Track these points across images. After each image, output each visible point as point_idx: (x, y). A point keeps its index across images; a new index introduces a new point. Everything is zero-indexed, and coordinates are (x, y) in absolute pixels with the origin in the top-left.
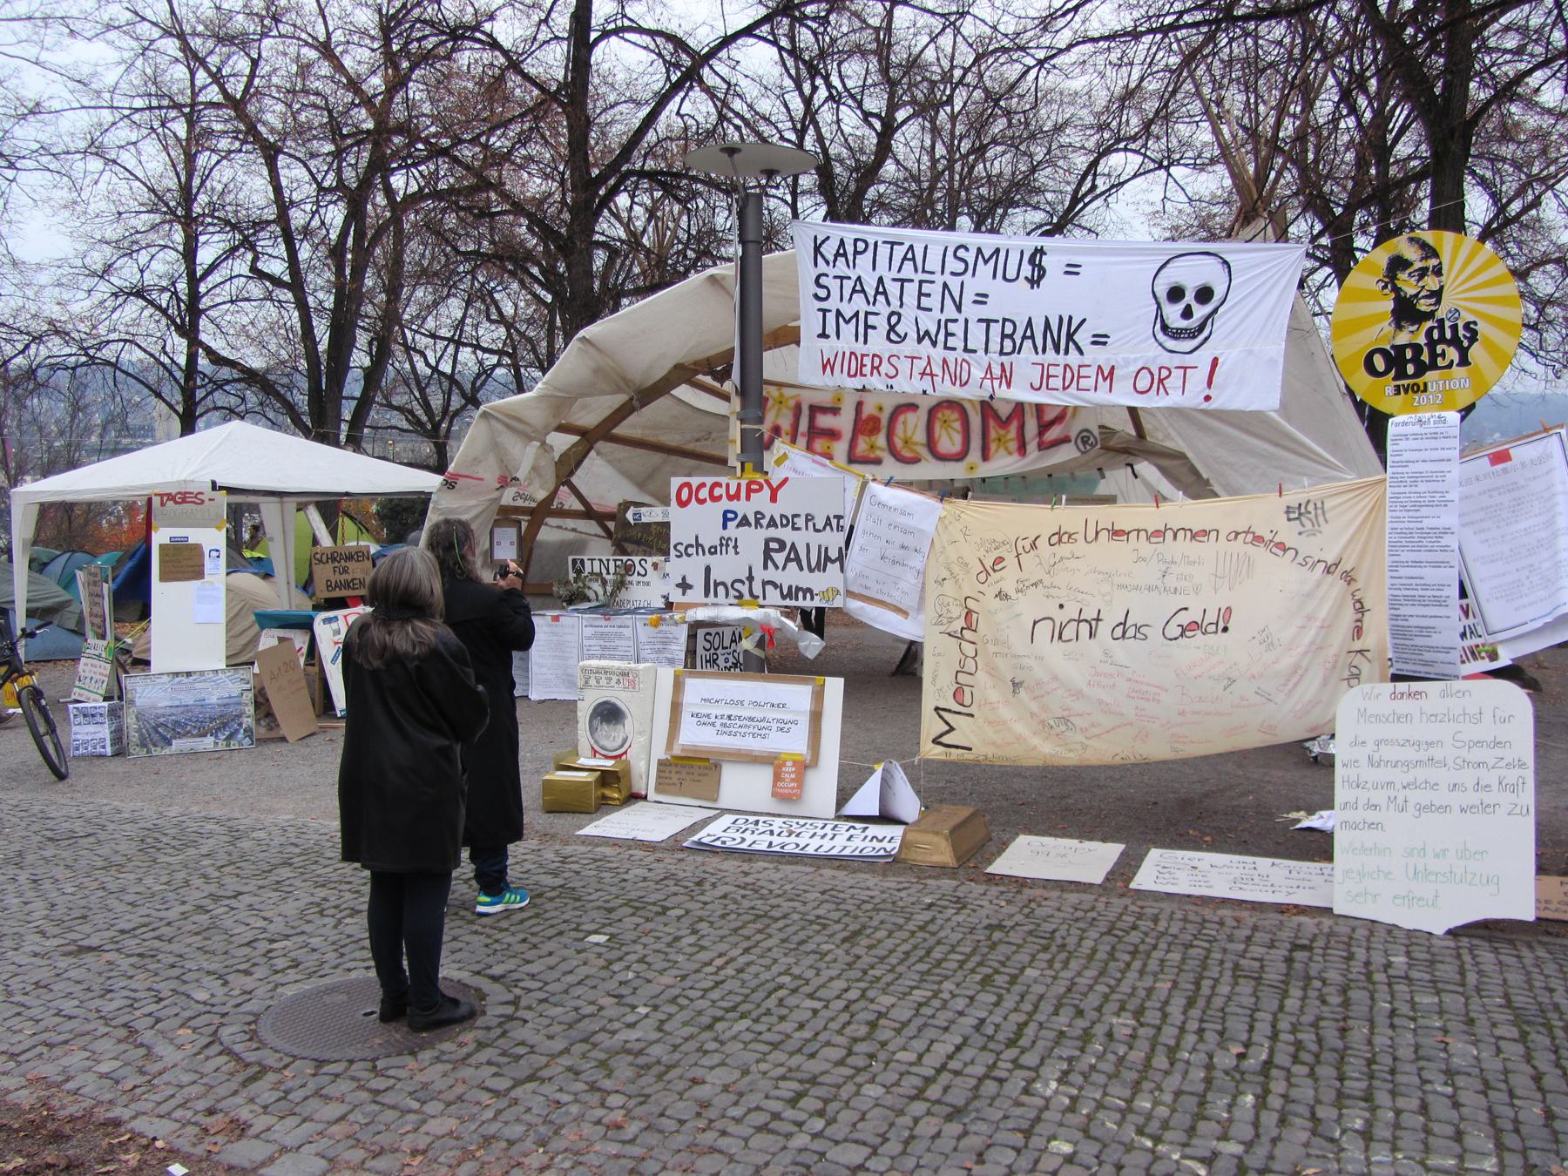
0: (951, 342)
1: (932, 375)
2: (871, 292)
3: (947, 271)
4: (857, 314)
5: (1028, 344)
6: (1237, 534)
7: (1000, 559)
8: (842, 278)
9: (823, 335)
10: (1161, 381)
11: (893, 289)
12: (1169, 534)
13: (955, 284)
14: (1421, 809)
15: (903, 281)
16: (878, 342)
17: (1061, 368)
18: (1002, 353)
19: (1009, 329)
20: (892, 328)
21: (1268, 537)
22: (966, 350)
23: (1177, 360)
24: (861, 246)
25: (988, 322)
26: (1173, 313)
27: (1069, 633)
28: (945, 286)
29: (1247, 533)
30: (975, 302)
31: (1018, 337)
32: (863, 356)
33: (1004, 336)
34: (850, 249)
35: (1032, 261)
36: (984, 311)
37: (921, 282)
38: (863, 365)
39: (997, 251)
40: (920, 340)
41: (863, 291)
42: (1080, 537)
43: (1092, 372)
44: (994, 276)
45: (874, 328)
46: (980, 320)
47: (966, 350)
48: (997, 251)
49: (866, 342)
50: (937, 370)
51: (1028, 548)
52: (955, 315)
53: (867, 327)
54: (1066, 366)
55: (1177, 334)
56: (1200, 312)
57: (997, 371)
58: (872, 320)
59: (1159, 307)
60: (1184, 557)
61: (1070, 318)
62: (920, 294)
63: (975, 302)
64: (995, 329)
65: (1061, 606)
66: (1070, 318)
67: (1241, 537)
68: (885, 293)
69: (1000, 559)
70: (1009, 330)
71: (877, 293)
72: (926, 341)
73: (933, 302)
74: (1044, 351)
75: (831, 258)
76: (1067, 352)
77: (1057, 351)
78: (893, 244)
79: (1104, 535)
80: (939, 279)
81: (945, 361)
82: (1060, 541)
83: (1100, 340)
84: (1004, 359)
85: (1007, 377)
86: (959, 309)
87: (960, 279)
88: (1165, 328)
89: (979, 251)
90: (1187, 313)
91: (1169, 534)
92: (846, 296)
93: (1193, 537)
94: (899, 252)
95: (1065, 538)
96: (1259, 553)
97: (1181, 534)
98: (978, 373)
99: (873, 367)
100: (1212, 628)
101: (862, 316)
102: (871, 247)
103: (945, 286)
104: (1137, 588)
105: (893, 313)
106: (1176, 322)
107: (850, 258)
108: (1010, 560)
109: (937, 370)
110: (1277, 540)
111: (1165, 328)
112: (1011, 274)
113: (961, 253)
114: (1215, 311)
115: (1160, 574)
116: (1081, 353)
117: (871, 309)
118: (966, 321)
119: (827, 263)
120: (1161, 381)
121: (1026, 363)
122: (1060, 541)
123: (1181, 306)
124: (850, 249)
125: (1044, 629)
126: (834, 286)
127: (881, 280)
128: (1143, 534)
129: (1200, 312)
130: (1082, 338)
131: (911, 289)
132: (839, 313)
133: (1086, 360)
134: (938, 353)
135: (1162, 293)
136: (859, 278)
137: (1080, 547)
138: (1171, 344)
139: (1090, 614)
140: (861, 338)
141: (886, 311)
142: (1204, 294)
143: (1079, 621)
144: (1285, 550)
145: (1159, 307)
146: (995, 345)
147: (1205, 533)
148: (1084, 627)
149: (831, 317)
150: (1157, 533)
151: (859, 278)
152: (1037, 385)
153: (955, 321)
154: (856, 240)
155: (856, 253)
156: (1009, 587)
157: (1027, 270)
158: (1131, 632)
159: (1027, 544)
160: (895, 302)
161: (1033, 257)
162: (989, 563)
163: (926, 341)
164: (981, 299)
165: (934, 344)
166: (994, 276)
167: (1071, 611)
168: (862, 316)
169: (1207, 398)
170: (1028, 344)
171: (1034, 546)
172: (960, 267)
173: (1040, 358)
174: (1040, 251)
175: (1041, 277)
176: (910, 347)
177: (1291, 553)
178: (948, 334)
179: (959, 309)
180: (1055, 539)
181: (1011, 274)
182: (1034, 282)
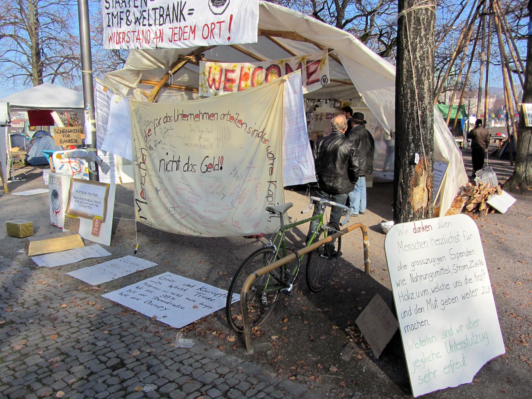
6: (224, 115)
7: (150, 130)
9: (109, 26)
10: (212, 31)
14: (445, 303)
61: (181, 2)
66: (181, 2)
67: (226, 117)
96: (232, 125)
100: (216, 167)
120: (212, 31)
130: (185, 12)
133: (186, 24)
139: (176, 159)
147: (213, 115)
159: (157, 122)
169: (229, 39)
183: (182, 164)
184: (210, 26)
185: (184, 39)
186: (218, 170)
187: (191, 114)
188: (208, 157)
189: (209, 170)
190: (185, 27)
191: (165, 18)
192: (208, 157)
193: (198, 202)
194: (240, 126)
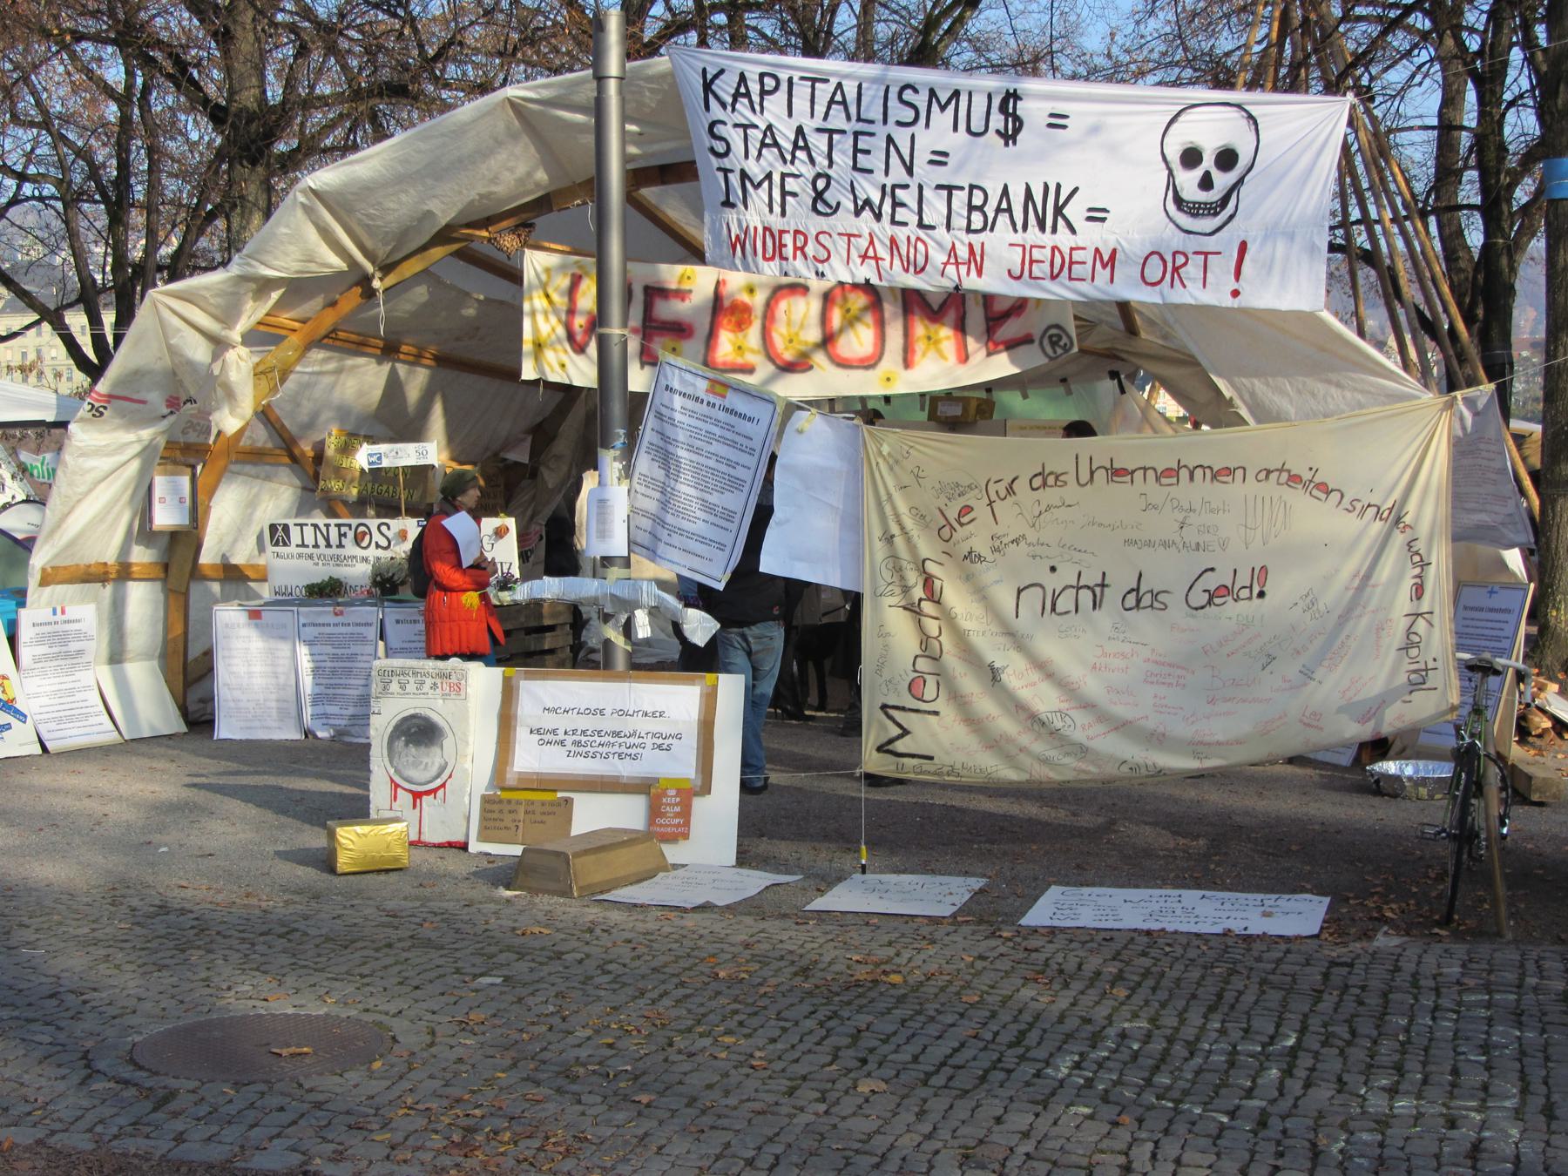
0: (901, 214)
1: (876, 259)
2: (787, 146)
3: (891, 120)
4: (769, 176)
5: (1003, 219)
6: (1269, 472)
7: (967, 509)
8: (745, 127)
9: (727, 203)
10: (1176, 269)
11: (819, 143)
12: (1184, 473)
13: (902, 137)
15: (831, 132)
16: (799, 214)
17: (1048, 252)
18: (969, 230)
19: (978, 199)
20: (819, 196)
21: (1307, 476)
22: (921, 225)
23: (1193, 243)
24: (769, 83)
25: (950, 189)
26: (1188, 181)
27: (1065, 603)
28: (890, 140)
29: (1280, 471)
30: (931, 162)
31: (990, 210)
32: (781, 232)
33: (971, 208)
34: (755, 88)
35: (1003, 108)
36: (942, 175)
37: (856, 134)
38: (782, 246)
39: (956, 94)
40: (858, 213)
41: (776, 144)
42: (1071, 478)
43: (1087, 256)
44: (955, 128)
45: (794, 195)
46: (939, 187)
47: (921, 225)
48: (956, 94)
49: (783, 214)
50: (883, 252)
51: (1003, 493)
52: (905, 179)
53: (784, 193)
54: (1054, 248)
55: (1195, 210)
56: (1222, 180)
57: (963, 253)
58: (791, 184)
59: (1171, 174)
60: (1204, 502)
61: (1058, 186)
62: (856, 150)
63: (931, 162)
64: (960, 198)
65: (1053, 569)
66: (1058, 186)
67: (1274, 476)
68: (806, 148)
69: (967, 509)
70: (977, 201)
71: (796, 146)
72: (867, 214)
73: (875, 161)
74: (1025, 227)
75: (729, 100)
76: (1054, 230)
77: (1042, 227)
78: (814, 81)
79: (1101, 475)
80: (881, 131)
81: (893, 241)
82: (1045, 484)
83: (1097, 216)
84: (973, 238)
85: (976, 260)
86: (910, 171)
87: (909, 131)
88: (1179, 201)
89: (932, 93)
90: (1206, 183)
91: (1184, 473)
92: (753, 152)
93: (1214, 477)
94: (824, 92)
95: (1051, 480)
97: (1198, 473)
98: (939, 257)
99: (796, 248)
100: (1245, 593)
101: (776, 178)
102: (784, 86)
103: (890, 140)
104: (1149, 544)
105: (819, 175)
106: (1191, 193)
107: (756, 99)
108: (981, 511)
109: (883, 252)
110: (1317, 479)
111: (1179, 201)
112: (977, 125)
113: (908, 95)
114: (1241, 181)
115: (1177, 525)
116: (1073, 231)
117: (789, 169)
118: (921, 188)
119: (724, 105)
120: (1176, 269)
121: (1002, 245)
122: (1045, 484)
123: (1197, 173)
124: (755, 88)
125: (1032, 598)
126: (735, 137)
127: (800, 131)
128: (1150, 473)
129: (1222, 180)
130: (1074, 211)
131: (844, 144)
132: (744, 175)
133: (1079, 240)
134: (885, 229)
135: (1174, 155)
136: (770, 127)
137: (1071, 491)
138: (1184, 220)
139: (1091, 578)
140: (777, 209)
141: (809, 172)
142: (1227, 159)
143: (1079, 588)
144: (1328, 492)
145: (1171, 174)
146: (959, 222)
147: (1229, 471)
148: (1086, 596)
149: (734, 179)
150: (1168, 472)
151: (770, 127)
152: (1018, 273)
153: (906, 187)
154: (762, 75)
155: (764, 93)
156: (981, 545)
157: (997, 121)
158: (1147, 600)
159: (1002, 488)
160: (822, 161)
161: (1004, 102)
162: (952, 514)
163: (867, 214)
164: (940, 158)
165: (878, 217)
166: (955, 128)
167: (1067, 576)
168: (776, 178)
170: (1003, 219)
171: (1010, 490)
172: (909, 115)
173: (1019, 237)
174: (1013, 96)
175: (1017, 131)
176: (844, 220)
177: (1335, 496)
178: (896, 204)
179: (910, 171)
180: (1037, 482)
181: (977, 125)
182: (1009, 137)
183: (1112, 596)
184: (1169, 259)
185: (1070, 279)
186: (1250, 598)
187: (1145, 469)
188: (1212, 569)
189: (1217, 601)
190: (1072, 249)
191: (991, 216)
192: (1212, 569)
193: (1182, 681)
194: (1323, 496)
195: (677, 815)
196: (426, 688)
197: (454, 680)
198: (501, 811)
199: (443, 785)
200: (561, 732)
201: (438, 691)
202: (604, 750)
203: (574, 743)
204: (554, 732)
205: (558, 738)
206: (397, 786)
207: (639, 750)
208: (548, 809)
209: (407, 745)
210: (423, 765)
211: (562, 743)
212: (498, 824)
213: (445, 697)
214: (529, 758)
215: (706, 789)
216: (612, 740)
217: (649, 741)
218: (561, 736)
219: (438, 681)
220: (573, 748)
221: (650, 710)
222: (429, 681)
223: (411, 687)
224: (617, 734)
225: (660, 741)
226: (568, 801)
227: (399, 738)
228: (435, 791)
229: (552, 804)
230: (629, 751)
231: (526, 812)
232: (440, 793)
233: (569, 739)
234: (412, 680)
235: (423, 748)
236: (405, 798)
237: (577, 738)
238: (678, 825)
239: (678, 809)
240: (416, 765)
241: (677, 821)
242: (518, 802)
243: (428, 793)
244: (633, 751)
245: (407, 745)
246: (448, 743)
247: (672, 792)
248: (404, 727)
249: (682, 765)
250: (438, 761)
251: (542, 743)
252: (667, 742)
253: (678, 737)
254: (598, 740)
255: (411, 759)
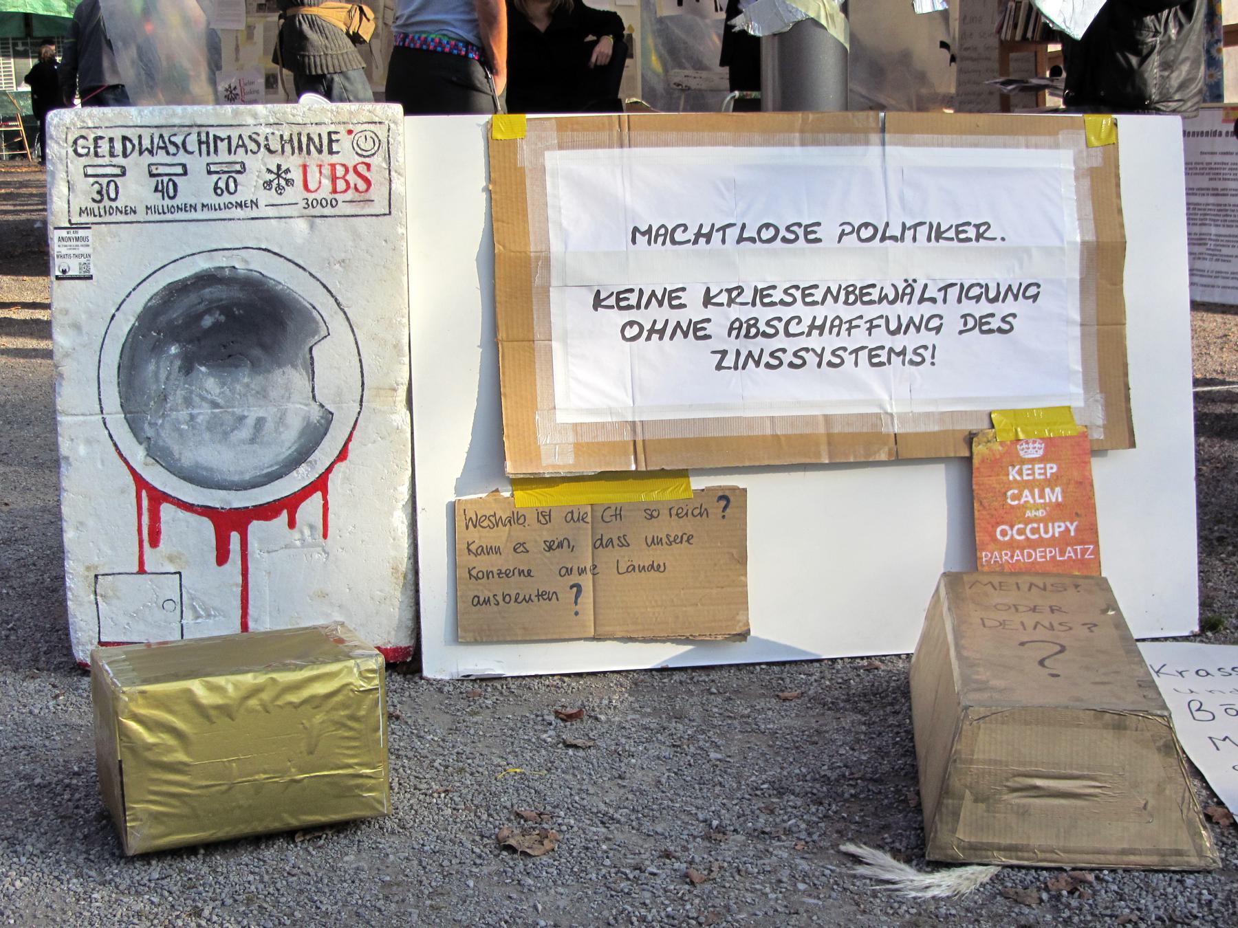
195: (1057, 512)
196: (249, 187)
197: (346, 155)
198: (520, 548)
199: (320, 484)
200: (693, 298)
201: (294, 193)
202: (829, 342)
203: (735, 328)
204: (671, 298)
205: (683, 317)
206: (158, 498)
207: (926, 338)
208: (666, 527)
209: (188, 368)
210: (234, 424)
211: (697, 330)
212: (514, 586)
213: (315, 210)
214: (594, 385)
215: (1122, 432)
216: (847, 313)
217: (952, 312)
218: (694, 311)
219: (292, 162)
220: (731, 345)
221: (947, 221)
222: (258, 165)
223: (196, 187)
224: (856, 294)
225: (983, 308)
226: (731, 501)
227: (157, 349)
228: (291, 504)
229: (679, 511)
230: (898, 342)
231: (600, 544)
232: (310, 509)
233: (719, 319)
234: (197, 164)
235: (244, 377)
236: (188, 535)
237: (745, 313)
238: (1063, 541)
239: (1055, 495)
240: (221, 429)
241: (1057, 529)
242: (574, 517)
243: (267, 512)
244: (910, 341)
245: (188, 368)
246: (332, 355)
247: (1034, 451)
248: (176, 314)
249: (1037, 369)
250: (299, 412)
251: (634, 333)
252: (1001, 309)
253: (1029, 292)
254: (807, 314)
255: (204, 413)
